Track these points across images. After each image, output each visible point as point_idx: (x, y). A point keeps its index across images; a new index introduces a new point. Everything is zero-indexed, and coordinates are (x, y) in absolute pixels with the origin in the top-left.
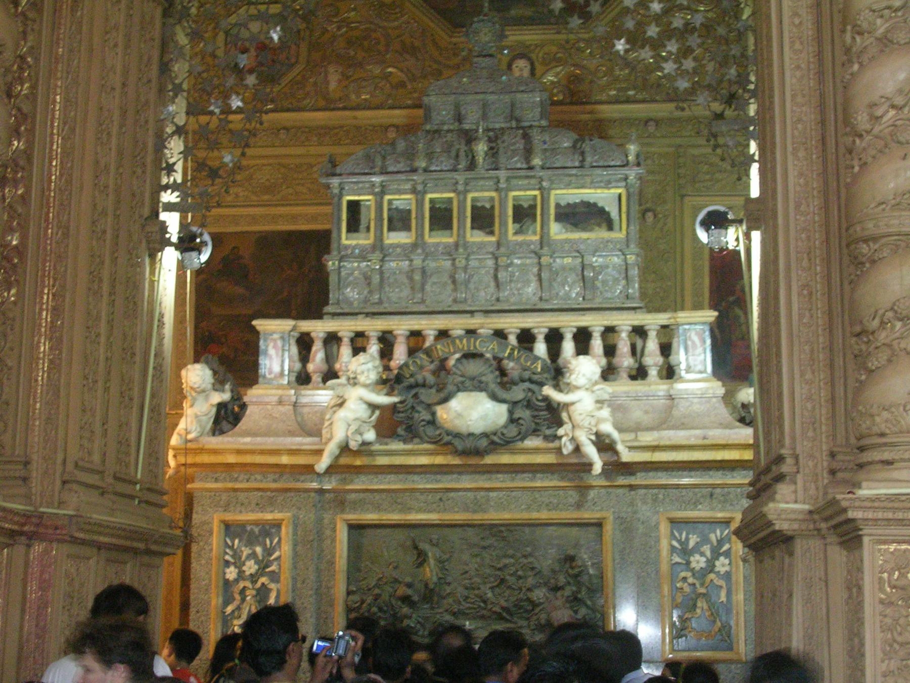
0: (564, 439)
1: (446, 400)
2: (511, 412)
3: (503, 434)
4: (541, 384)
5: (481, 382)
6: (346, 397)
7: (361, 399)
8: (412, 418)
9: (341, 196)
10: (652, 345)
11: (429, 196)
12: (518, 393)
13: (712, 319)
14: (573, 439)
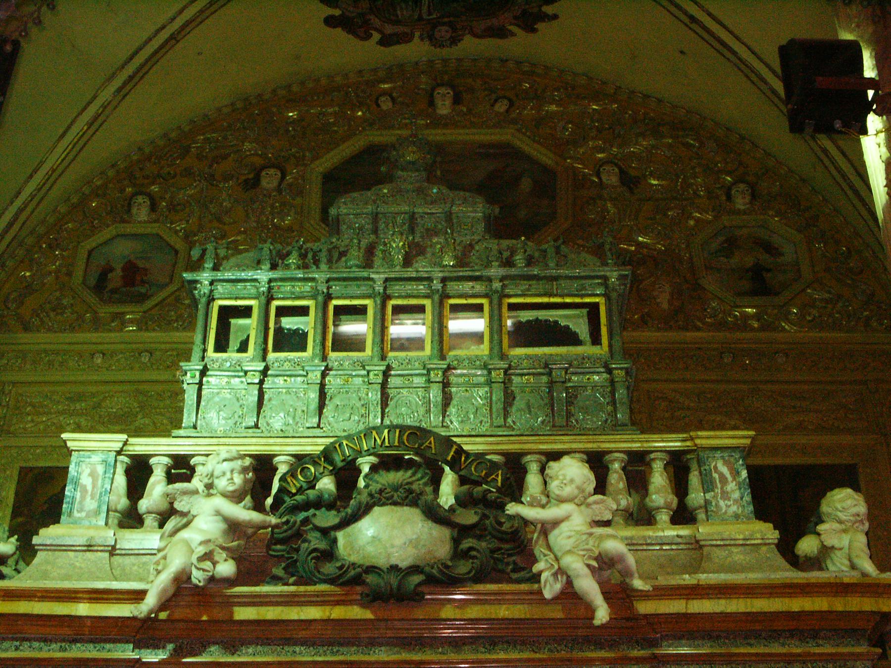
0: (544, 576)
1: (355, 517)
2: (456, 541)
3: (447, 567)
4: (502, 507)
5: (410, 492)
6: (193, 512)
7: (218, 513)
8: (297, 550)
9: (211, 299)
10: (659, 479)
11: (335, 302)
12: (469, 517)
13: (748, 441)
14: (560, 571)
